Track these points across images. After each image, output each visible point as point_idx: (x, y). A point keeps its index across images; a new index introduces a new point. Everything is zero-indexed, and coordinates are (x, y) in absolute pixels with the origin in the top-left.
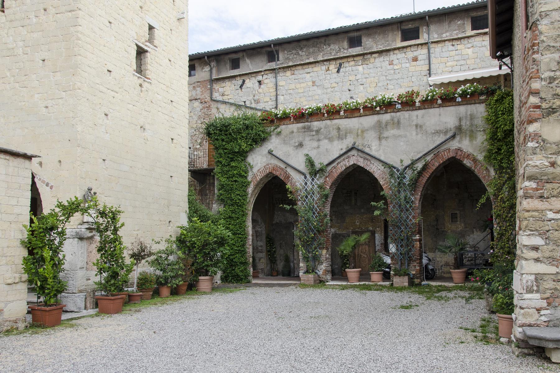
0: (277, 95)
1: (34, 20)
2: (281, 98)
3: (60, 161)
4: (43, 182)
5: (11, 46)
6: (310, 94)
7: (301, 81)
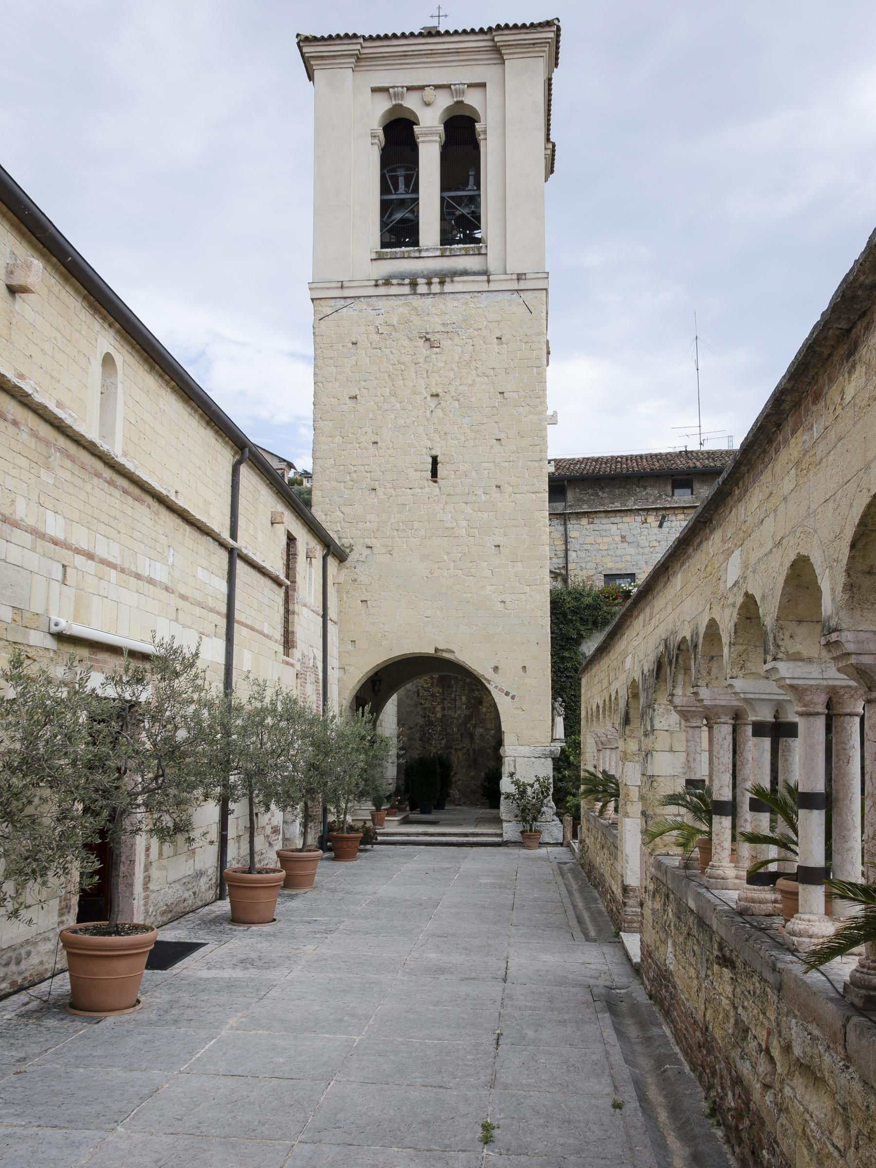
0: (566, 550)
1: (483, 497)
2: (572, 555)
3: (524, 667)
4: (501, 690)
5: (450, 525)
6: (618, 552)
7: (604, 534)
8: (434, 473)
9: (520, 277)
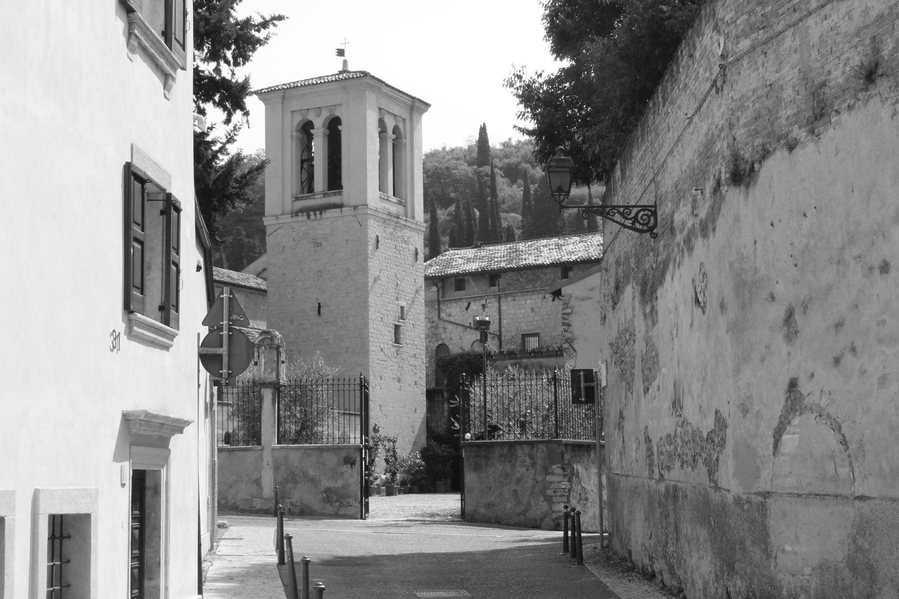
0: (500, 319)
2: (504, 322)
8: (319, 313)
9: (355, 207)
